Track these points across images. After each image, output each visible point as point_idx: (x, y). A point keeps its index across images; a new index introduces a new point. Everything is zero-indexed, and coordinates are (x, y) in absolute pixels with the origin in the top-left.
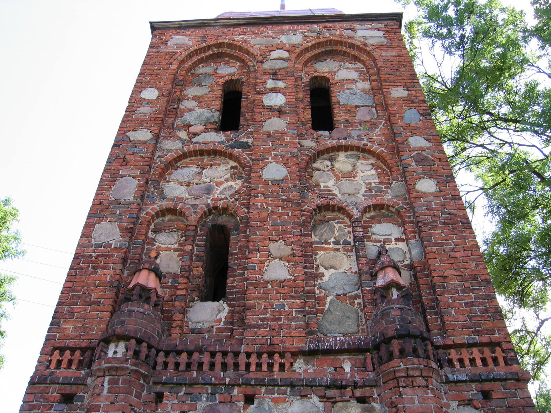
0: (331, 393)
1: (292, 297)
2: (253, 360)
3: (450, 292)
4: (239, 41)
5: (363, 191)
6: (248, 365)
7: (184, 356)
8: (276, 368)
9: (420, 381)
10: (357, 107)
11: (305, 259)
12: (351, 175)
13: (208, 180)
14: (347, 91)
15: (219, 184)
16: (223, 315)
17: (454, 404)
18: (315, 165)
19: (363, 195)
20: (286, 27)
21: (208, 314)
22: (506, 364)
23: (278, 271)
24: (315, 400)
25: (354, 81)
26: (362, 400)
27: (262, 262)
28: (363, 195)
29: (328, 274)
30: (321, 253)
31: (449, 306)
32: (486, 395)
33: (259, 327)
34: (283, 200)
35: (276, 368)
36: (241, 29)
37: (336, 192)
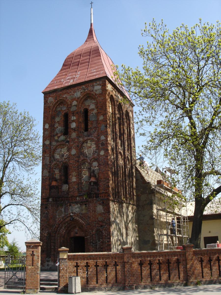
0: (81, 203)
1: (76, 185)
2: (70, 198)
3: (102, 182)
4: (64, 98)
5: (92, 153)
6: (70, 199)
7: (61, 198)
8: (74, 199)
9: (92, 202)
10: (93, 121)
11: (79, 176)
12: (90, 147)
13: (63, 153)
14: (92, 115)
15: (65, 153)
16: (67, 188)
17: (98, 204)
18: (83, 145)
19: (92, 154)
20: (76, 88)
21: (65, 187)
22: (108, 197)
23: (74, 179)
24: (79, 205)
25: (94, 109)
26: (86, 204)
27: (71, 177)
28: (92, 154)
29: (84, 176)
30: (83, 171)
31: (101, 185)
32: (103, 203)
33: (71, 192)
34: (75, 161)
35: (74, 199)
36: (65, 91)
37: (87, 153)
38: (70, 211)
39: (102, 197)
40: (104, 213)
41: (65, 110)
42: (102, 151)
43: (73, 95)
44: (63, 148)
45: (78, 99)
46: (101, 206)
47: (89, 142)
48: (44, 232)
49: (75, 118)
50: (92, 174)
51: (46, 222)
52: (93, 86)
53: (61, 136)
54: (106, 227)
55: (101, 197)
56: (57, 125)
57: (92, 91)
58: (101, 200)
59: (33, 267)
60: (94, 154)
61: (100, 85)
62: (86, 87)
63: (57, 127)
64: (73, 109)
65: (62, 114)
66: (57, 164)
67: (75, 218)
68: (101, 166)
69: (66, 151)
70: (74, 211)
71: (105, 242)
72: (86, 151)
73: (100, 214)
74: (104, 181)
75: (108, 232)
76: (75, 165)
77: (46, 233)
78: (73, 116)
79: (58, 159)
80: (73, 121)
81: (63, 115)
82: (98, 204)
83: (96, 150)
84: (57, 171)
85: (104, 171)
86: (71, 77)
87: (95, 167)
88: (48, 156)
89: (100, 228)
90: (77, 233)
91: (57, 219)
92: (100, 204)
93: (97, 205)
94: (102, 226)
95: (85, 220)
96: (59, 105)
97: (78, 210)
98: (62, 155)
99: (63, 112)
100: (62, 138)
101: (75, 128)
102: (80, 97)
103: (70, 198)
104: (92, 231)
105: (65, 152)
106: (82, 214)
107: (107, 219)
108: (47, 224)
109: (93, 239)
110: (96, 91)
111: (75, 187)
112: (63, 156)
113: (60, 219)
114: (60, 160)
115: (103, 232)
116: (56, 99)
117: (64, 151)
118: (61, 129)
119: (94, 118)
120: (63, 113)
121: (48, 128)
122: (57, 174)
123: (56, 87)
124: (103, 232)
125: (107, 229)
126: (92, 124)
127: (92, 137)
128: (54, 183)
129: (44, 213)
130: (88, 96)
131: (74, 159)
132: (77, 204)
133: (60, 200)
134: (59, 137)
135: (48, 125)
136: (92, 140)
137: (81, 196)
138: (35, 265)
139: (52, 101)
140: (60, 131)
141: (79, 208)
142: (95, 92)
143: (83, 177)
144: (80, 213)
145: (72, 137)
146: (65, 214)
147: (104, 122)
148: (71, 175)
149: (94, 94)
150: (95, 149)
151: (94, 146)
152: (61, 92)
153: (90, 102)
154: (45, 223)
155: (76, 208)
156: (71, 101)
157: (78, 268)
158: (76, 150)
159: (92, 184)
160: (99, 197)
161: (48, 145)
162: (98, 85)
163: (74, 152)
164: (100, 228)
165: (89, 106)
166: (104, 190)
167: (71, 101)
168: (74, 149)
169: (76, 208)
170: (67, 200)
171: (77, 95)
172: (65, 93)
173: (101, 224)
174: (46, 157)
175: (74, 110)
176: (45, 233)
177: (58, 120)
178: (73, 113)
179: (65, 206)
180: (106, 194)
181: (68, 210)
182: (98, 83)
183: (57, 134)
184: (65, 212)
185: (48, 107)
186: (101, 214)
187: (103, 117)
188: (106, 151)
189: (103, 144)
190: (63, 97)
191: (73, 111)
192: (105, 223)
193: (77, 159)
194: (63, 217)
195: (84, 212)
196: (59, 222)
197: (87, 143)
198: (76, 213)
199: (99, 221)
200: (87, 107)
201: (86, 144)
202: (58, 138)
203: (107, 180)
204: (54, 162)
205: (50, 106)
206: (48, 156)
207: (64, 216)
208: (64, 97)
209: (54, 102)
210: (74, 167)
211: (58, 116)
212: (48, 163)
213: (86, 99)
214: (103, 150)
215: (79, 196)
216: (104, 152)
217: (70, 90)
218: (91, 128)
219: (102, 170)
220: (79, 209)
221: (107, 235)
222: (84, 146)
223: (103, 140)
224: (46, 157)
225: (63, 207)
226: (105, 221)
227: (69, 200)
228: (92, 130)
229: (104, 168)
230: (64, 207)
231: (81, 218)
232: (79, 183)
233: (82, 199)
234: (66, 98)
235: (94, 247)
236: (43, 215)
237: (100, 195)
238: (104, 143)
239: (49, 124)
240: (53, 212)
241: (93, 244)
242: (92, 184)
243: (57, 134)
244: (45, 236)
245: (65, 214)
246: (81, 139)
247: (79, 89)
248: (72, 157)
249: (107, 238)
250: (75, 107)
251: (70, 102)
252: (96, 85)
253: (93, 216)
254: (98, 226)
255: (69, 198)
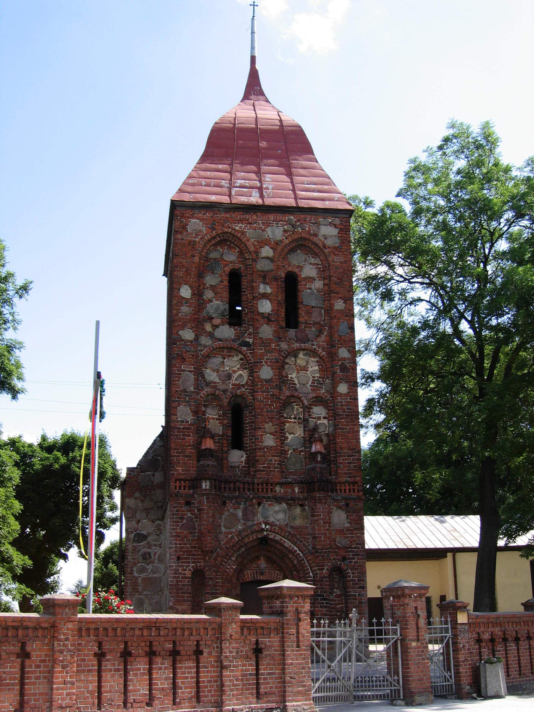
0: (290, 502)
1: (276, 456)
2: (260, 487)
3: (342, 456)
4: (238, 231)
5: (310, 383)
6: (258, 489)
7: (232, 484)
8: (269, 491)
9: (324, 501)
10: (313, 307)
11: (280, 434)
12: (305, 369)
13: (228, 368)
14: (308, 291)
15: (235, 372)
16: (243, 459)
17: (335, 508)
18: (286, 361)
19: (311, 386)
20: (272, 217)
21: (237, 457)
22: (358, 492)
23: (269, 441)
24: (284, 505)
25: (313, 279)
26: (301, 505)
27: (262, 435)
28: (311, 386)
29: (290, 437)
30: (287, 424)
31: (341, 463)
32: (347, 505)
33: (262, 471)
34: (271, 395)
35: (269, 491)
36: (238, 215)
37: (296, 382)
38: (260, 518)
39: (345, 492)
40: (350, 530)
41: (231, 262)
42: (341, 384)
43: (263, 231)
44: (229, 356)
45: (275, 245)
46: (342, 511)
47: (301, 355)
48: (183, 566)
49: (269, 290)
50: (311, 435)
51: (188, 540)
52: (318, 224)
53: (223, 325)
54: (356, 562)
55: (341, 492)
56: (209, 294)
57: (316, 235)
58: (344, 498)
59: (419, 644)
60: (315, 388)
61: (335, 226)
62: (298, 221)
63: (210, 301)
64: (262, 265)
65: (224, 271)
66: (214, 395)
67: (270, 537)
68: (341, 418)
69: (238, 366)
70: (272, 519)
71: (353, 595)
72: (294, 375)
73: (341, 532)
74: (348, 456)
75: (360, 573)
76: (270, 405)
77: (190, 570)
78: (265, 283)
79: (215, 383)
80: (265, 296)
81: (227, 273)
82: (335, 508)
83: (320, 378)
84: (212, 414)
85: (348, 432)
86: (249, 184)
87: (319, 418)
88: (191, 372)
89: (341, 564)
90: (262, 574)
91: (221, 536)
92: (340, 508)
93: (332, 509)
94: (344, 559)
95: (301, 542)
96: (215, 245)
97: (281, 516)
98: (226, 373)
99: (226, 265)
100: (226, 332)
101: (269, 314)
102: (281, 241)
103: (260, 487)
104: (319, 569)
105: (236, 369)
106: (292, 527)
107: (358, 544)
108: (192, 547)
109: (323, 588)
110: (325, 238)
111: (272, 461)
112: (229, 377)
113: (230, 536)
114: (222, 387)
115: (349, 573)
116: (213, 229)
117: (233, 363)
118: (222, 308)
119: (316, 300)
120: (227, 269)
121: (191, 299)
122: (211, 421)
123: (213, 198)
124: (349, 573)
125: (359, 566)
126: (309, 313)
127: (313, 345)
128: (208, 444)
129: (182, 518)
130: (304, 244)
131: (270, 392)
132: (280, 503)
133: (230, 488)
134: (217, 326)
135: (190, 291)
136: (312, 353)
137: (290, 483)
138: (421, 640)
139: (201, 231)
140: (220, 311)
141: (285, 512)
142: (323, 239)
143: (287, 438)
144: (287, 525)
145: (261, 335)
146: (244, 524)
147: (346, 316)
148: (260, 428)
149: (321, 245)
150: (318, 375)
151: (314, 368)
152: (228, 215)
153: (303, 258)
154: (185, 544)
155: (276, 512)
156: (256, 243)
157: (178, 658)
158: (272, 369)
159: (319, 459)
160: (337, 492)
161: (191, 341)
162: (330, 224)
163: (266, 372)
164: (341, 564)
165: (300, 268)
166: (349, 477)
167: (256, 243)
168: (268, 366)
169: (276, 512)
170: (249, 490)
171: (273, 232)
172: (241, 221)
173: (343, 553)
174: (184, 371)
175: (266, 269)
176: (185, 570)
177: (213, 284)
178: (264, 277)
179: (245, 504)
180: (354, 486)
181: (254, 515)
182: (330, 220)
183: (211, 319)
184: (246, 517)
185: (190, 242)
186: (343, 530)
187: (344, 305)
188: (353, 386)
189: (343, 368)
190: (235, 230)
191: (262, 272)
192: (354, 552)
193: (276, 391)
194: (240, 533)
195: (298, 522)
196: (226, 543)
197: (296, 356)
198: (278, 523)
199: (339, 548)
200: (297, 270)
201: (293, 359)
202: (214, 330)
203: (356, 452)
204: (207, 390)
205: (195, 241)
206: (191, 372)
207: (244, 530)
208: (237, 228)
209: (205, 235)
210: (267, 411)
211: (213, 273)
212: (192, 389)
213: (293, 250)
214: (346, 382)
215: (282, 484)
216: (348, 388)
217: (255, 217)
218: (306, 323)
219: (343, 429)
220: (286, 515)
221: (358, 580)
222: (287, 363)
223: (344, 359)
224: (184, 371)
225: (239, 508)
226: (352, 548)
227: (256, 491)
228: (308, 327)
229: (348, 425)
230: (242, 506)
231: (291, 537)
232: (281, 451)
233: (290, 490)
234: (243, 233)
235: (325, 607)
236: (178, 522)
237: (338, 488)
238: (348, 365)
239: (191, 288)
240: (214, 516)
241: (325, 599)
242: (319, 459)
243: (211, 319)
244: (186, 578)
245: (244, 524)
246: (284, 346)
247: (282, 221)
248: (262, 385)
249: (358, 588)
250: (267, 262)
251: (254, 246)
252: (326, 223)
253: (326, 534)
254: (334, 559)
255: (256, 486)
